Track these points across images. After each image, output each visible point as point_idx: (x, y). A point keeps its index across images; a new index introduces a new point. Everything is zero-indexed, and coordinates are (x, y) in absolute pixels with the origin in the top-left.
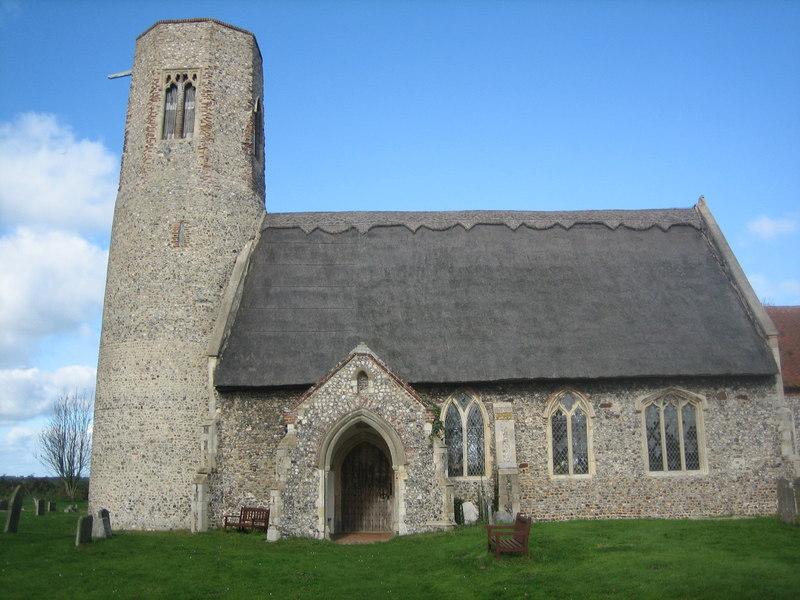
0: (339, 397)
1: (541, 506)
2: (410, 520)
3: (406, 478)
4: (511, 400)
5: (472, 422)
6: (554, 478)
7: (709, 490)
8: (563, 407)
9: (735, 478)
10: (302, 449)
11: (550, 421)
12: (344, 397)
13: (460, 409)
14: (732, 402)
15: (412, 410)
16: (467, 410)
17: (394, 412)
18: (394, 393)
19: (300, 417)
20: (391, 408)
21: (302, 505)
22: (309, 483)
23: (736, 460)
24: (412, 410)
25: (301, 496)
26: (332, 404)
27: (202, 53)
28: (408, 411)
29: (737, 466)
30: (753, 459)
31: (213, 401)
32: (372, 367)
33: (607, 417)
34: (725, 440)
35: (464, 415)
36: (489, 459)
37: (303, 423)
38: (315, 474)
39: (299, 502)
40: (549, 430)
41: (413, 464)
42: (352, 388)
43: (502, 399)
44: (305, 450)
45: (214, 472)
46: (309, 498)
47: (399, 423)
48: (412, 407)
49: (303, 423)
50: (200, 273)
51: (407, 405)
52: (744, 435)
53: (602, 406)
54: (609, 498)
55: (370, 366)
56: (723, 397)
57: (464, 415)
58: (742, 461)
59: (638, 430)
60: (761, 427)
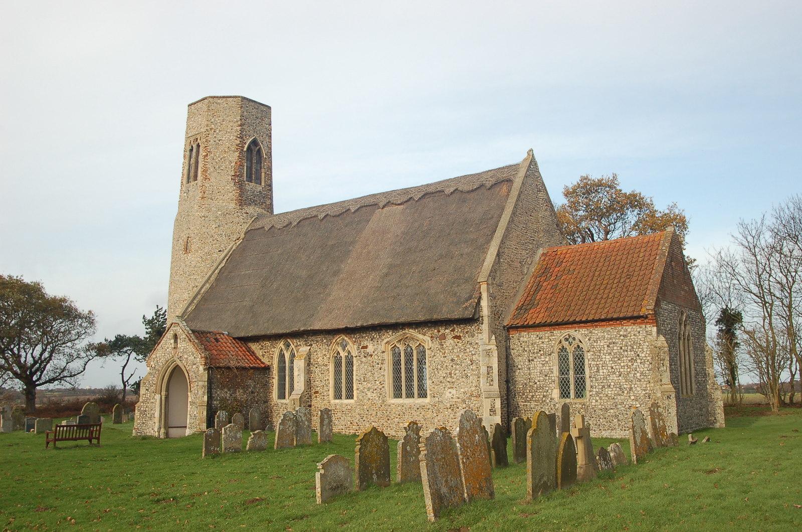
0: (166, 350)
4: (311, 345)
6: (334, 402)
7: (429, 415)
8: (340, 349)
9: (448, 406)
10: (151, 382)
13: (285, 352)
14: (449, 342)
19: (152, 363)
20: (186, 356)
23: (450, 390)
27: (205, 122)
28: (193, 358)
29: (450, 395)
30: (462, 390)
33: (365, 357)
34: (442, 373)
37: (153, 366)
40: (331, 367)
46: (152, 412)
48: (195, 355)
50: (196, 269)
51: (193, 354)
52: (456, 370)
53: (363, 347)
54: (364, 418)
56: (443, 337)
57: (287, 356)
58: (453, 391)
59: (383, 366)
60: (469, 362)
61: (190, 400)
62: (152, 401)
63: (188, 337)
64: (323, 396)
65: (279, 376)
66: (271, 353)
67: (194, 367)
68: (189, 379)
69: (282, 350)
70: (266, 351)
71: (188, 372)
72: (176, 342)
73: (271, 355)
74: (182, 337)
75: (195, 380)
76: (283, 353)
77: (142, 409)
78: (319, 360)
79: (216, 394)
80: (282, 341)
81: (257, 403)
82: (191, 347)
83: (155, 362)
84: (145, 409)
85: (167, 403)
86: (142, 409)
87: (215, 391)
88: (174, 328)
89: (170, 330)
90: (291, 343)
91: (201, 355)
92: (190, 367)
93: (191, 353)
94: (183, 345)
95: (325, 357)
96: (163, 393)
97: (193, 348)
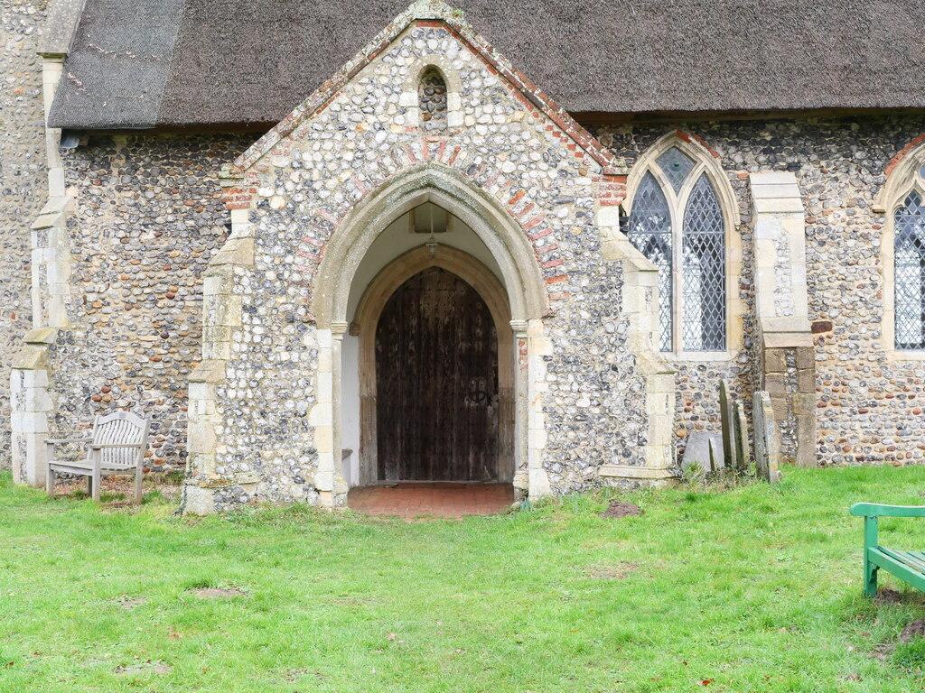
1: (859, 428)
2: (560, 460)
3: (549, 351)
5: (692, 223)
6: (894, 356)
10: (271, 275)
11: (890, 216)
12: (381, 136)
13: (668, 189)
15: (563, 173)
16: (687, 190)
17: (515, 178)
20: (508, 167)
21: (272, 421)
22: (290, 365)
24: (563, 173)
25: (270, 396)
26: (349, 156)
28: (554, 174)
31: (57, 172)
32: (453, 58)
35: (678, 202)
36: (735, 308)
37: (276, 204)
38: (307, 340)
39: (263, 414)
41: (566, 314)
42: (404, 111)
43: (772, 164)
44: (279, 277)
45: (66, 339)
46: (290, 404)
47: (528, 207)
48: (563, 164)
49: (276, 204)
51: (551, 159)
55: (452, 52)
57: (678, 202)
62: (285, 356)
64: (855, 338)
67: (563, 211)
74: (476, 83)
75: (573, 266)
77: (231, 394)
78: (830, 219)
84: (241, 394)
86: (231, 394)
88: (420, 44)
92: (536, 210)
93: (536, 156)
95: (857, 209)
97: (549, 135)
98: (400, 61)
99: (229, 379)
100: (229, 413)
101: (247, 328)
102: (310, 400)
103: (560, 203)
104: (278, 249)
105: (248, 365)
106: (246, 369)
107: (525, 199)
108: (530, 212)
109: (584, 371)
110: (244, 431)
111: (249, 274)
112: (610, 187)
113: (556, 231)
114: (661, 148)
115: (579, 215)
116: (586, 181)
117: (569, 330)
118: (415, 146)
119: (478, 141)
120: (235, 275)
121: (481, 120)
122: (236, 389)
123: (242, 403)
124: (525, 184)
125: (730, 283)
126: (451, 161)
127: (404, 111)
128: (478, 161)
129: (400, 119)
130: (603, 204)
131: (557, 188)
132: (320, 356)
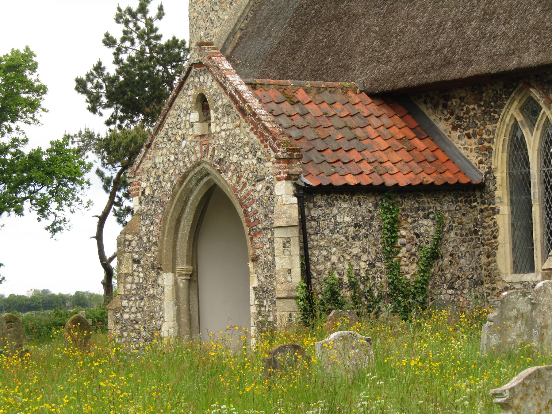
0: (179, 143)
10: (145, 239)
13: (526, 131)
15: (260, 160)
18: (238, 131)
19: (144, 185)
20: (234, 158)
22: (154, 297)
26: (172, 158)
28: (255, 161)
37: (147, 193)
47: (245, 185)
48: (259, 154)
55: (209, 84)
61: (254, 283)
62: (151, 292)
63: (236, 102)
65: (512, 203)
66: (485, 136)
67: (260, 186)
68: (248, 221)
69: (516, 126)
70: (471, 131)
71: (242, 204)
72: (205, 118)
73: (486, 144)
74: (220, 103)
76: (519, 135)
77: (126, 316)
79: (329, 264)
80: (514, 100)
81: (451, 287)
82: (248, 129)
83: (151, 180)
84: (133, 316)
85: (194, 298)
86: (126, 316)
87: (325, 253)
88: (197, 80)
89: (185, 86)
90: (541, 104)
91: (275, 151)
92: (249, 187)
93: (247, 149)
94: (224, 127)
96: (183, 267)
98: (189, 93)
99: (124, 307)
100: (124, 328)
101: (136, 274)
102: (162, 319)
103: (259, 181)
104: (148, 222)
105: (137, 298)
106: (136, 300)
107: (243, 180)
108: (245, 189)
109: (270, 297)
110: (135, 340)
111: (137, 239)
112: (280, 168)
113: (257, 201)
114: (518, 99)
115: (267, 188)
116: (269, 164)
117: (264, 269)
118: (197, 148)
119: (222, 142)
120: (126, 240)
121: (223, 128)
122: (130, 313)
123: (134, 322)
124: (243, 170)
125: (535, 217)
126: (212, 156)
127: (192, 126)
128: (222, 157)
129: (191, 132)
130: (279, 179)
131: (256, 171)
132: (166, 290)
